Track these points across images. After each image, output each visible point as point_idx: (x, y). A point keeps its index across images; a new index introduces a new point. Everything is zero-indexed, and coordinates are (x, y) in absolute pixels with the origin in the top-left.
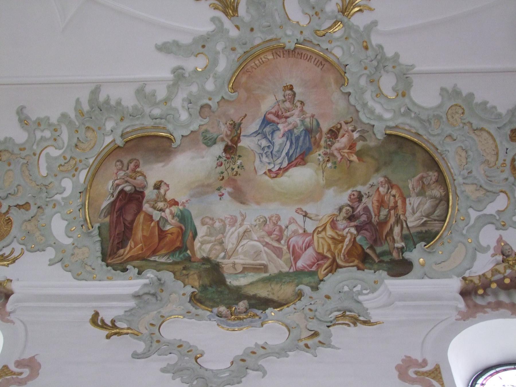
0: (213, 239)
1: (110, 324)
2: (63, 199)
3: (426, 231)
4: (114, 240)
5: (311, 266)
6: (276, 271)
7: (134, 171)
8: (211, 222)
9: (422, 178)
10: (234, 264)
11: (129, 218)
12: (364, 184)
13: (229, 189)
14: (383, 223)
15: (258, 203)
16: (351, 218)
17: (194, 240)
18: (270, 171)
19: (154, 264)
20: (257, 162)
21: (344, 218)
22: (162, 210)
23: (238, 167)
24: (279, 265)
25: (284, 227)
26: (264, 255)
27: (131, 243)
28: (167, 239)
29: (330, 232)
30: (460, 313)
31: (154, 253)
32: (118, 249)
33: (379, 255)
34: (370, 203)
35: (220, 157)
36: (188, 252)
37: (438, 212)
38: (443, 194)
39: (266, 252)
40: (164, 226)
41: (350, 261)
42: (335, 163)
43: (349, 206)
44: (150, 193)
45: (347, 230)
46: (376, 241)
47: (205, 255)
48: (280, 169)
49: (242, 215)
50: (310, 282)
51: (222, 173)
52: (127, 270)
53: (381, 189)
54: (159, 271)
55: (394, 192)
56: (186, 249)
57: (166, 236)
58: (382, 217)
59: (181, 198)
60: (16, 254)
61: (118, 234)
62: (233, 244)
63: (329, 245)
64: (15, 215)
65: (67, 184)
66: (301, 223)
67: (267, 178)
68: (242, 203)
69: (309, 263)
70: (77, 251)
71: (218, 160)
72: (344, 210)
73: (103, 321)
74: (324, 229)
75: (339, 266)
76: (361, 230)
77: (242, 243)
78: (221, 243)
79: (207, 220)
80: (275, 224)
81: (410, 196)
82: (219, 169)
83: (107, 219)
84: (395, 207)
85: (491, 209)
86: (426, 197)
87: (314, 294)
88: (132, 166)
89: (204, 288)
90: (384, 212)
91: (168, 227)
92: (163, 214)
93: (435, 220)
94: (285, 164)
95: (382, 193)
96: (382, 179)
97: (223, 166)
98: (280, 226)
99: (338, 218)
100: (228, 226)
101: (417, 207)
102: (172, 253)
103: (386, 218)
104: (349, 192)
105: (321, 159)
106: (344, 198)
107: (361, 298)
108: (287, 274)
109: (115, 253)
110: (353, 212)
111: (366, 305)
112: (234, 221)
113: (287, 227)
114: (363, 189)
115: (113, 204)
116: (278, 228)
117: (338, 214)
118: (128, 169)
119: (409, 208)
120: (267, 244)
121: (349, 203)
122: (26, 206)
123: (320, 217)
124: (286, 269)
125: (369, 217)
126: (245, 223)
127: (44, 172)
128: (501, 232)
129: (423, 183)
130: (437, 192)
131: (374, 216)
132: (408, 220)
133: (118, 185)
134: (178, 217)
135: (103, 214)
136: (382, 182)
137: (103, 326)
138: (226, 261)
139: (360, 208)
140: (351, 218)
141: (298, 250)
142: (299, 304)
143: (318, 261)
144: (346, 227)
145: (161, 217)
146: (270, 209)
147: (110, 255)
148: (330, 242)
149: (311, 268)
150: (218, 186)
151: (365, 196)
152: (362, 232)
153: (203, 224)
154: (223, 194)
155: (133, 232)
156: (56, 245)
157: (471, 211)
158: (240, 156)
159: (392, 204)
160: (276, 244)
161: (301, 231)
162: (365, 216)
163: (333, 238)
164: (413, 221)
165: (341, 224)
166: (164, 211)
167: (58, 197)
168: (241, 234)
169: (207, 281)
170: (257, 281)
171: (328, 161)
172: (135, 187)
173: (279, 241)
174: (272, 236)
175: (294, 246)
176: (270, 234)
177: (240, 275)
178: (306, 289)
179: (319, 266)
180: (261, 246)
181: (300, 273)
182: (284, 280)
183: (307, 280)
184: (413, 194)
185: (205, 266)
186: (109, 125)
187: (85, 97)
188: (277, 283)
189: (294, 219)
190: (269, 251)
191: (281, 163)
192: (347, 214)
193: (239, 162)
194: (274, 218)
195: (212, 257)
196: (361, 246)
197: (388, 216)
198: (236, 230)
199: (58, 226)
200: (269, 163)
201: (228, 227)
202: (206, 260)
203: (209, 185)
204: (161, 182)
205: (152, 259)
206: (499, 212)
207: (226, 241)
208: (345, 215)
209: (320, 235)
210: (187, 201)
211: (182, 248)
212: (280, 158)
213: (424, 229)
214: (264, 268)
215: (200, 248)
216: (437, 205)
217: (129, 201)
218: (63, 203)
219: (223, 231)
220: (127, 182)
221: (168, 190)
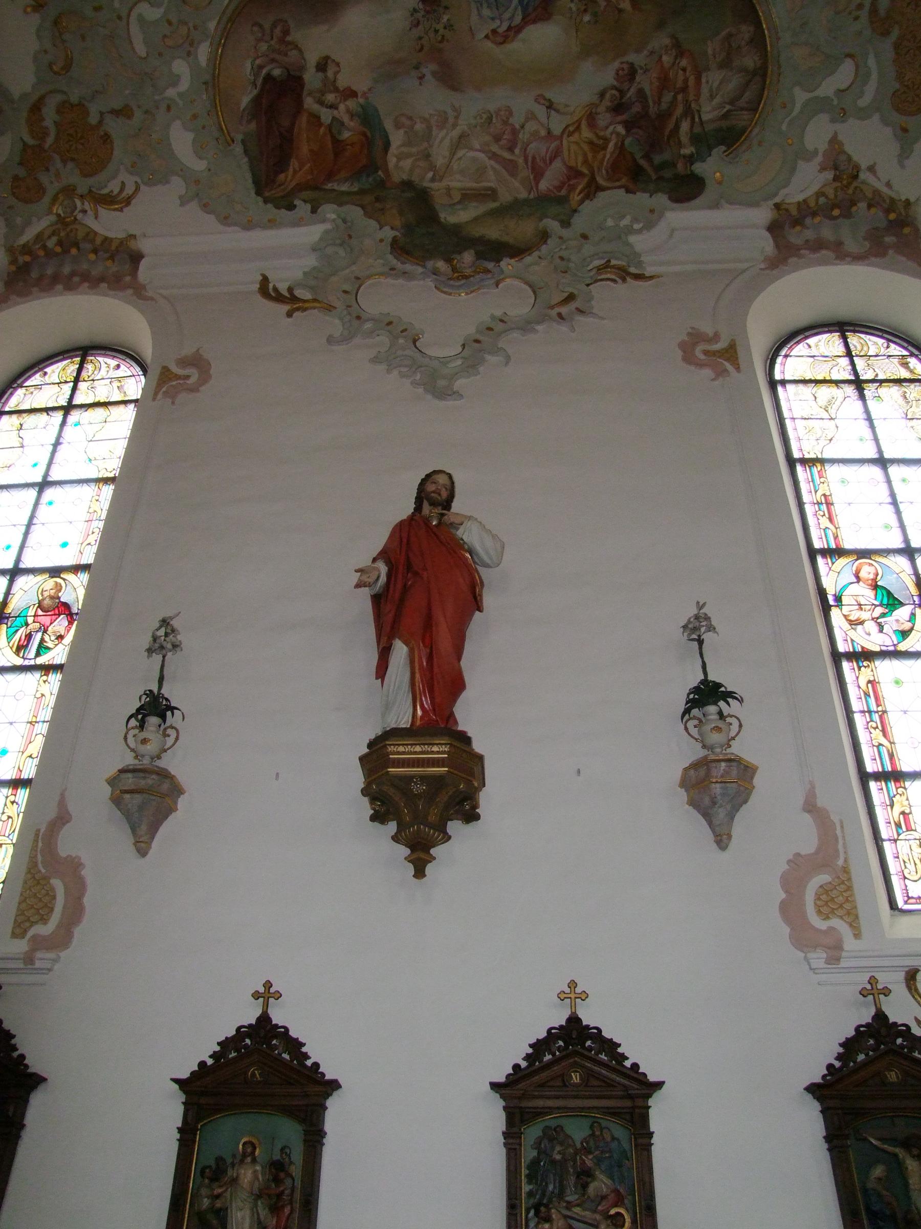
2: (180, 95)
7: (282, 41)
8: (408, 123)
9: (730, 35)
10: (449, 189)
12: (638, 51)
13: (433, 67)
14: (663, 116)
16: (618, 108)
18: (494, 31)
20: (474, 18)
21: (609, 110)
22: (333, 107)
23: (445, 28)
24: (514, 189)
25: (517, 127)
26: (491, 173)
27: (294, 163)
29: (586, 133)
31: (330, 176)
34: (646, 82)
35: (415, 10)
36: (380, 173)
37: (748, 95)
40: (340, 133)
42: (595, 15)
44: (311, 78)
45: (611, 128)
47: (405, 177)
48: (510, 28)
49: (454, 109)
51: (420, 38)
53: (665, 58)
55: (684, 62)
56: (377, 169)
58: (664, 106)
59: (361, 86)
60: (129, 190)
63: (585, 155)
64: (113, 126)
65: (180, 67)
67: (489, 44)
68: (454, 88)
69: (556, 183)
71: (412, 15)
72: (608, 96)
74: (578, 128)
77: (456, 157)
78: (428, 156)
79: (403, 120)
80: (505, 123)
81: (707, 69)
82: (416, 32)
83: (253, 126)
84: (684, 89)
85: (827, 88)
88: (278, 31)
90: (667, 97)
91: (346, 135)
92: (335, 112)
93: (742, 109)
94: (518, 19)
95: (666, 65)
96: (667, 41)
97: (420, 27)
99: (599, 110)
100: (434, 128)
104: (616, 64)
105: (574, 9)
106: (607, 77)
108: (526, 202)
110: (622, 98)
112: (443, 122)
113: (522, 127)
114: (638, 59)
115: (257, 100)
117: (597, 102)
118: (272, 38)
119: (705, 90)
120: (494, 156)
121: (615, 83)
123: (572, 109)
124: (523, 195)
125: (645, 106)
126: (460, 122)
127: (141, 49)
128: (838, 127)
129: (730, 46)
130: (750, 61)
131: (651, 104)
132: (703, 109)
133: (261, 67)
134: (359, 117)
136: (667, 46)
138: (435, 185)
139: (632, 92)
140: (618, 108)
141: (542, 165)
143: (569, 180)
144: (610, 124)
145: (334, 118)
148: (586, 147)
149: (560, 191)
151: (639, 71)
152: (634, 130)
153: (398, 126)
154: (424, 76)
157: (797, 91)
158: (446, 8)
159: (679, 84)
160: (506, 155)
161: (543, 133)
163: (591, 143)
164: (709, 111)
165: (603, 119)
166: (337, 108)
167: (171, 93)
171: (585, 11)
173: (511, 149)
174: (503, 142)
175: (534, 158)
176: (497, 139)
177: (459, 207)
178: (552, 225)
179: (572, 188)
180: (486, 159)
189: (532, 113)
190: (497, 166)
191: (511, 18)
193: (445, 18)
194: (502, 113)
195: (415, 179)
198: (447, 134)
199: (182, 141)
200: (493, 19)
202: (407, 185)
204: (327, 58)
205: (329, 186)
206: (840, 92)
208: (609, 104)
209: (572, 139)
210: (370, 90)
212: (510, 10)
213: (724, 124)
214: (491, 194)
216: (747, 84)
217: (280, 94)
218: (181, 103)
219: (428, 136)
220: (273, 60)
221: (338, 72)
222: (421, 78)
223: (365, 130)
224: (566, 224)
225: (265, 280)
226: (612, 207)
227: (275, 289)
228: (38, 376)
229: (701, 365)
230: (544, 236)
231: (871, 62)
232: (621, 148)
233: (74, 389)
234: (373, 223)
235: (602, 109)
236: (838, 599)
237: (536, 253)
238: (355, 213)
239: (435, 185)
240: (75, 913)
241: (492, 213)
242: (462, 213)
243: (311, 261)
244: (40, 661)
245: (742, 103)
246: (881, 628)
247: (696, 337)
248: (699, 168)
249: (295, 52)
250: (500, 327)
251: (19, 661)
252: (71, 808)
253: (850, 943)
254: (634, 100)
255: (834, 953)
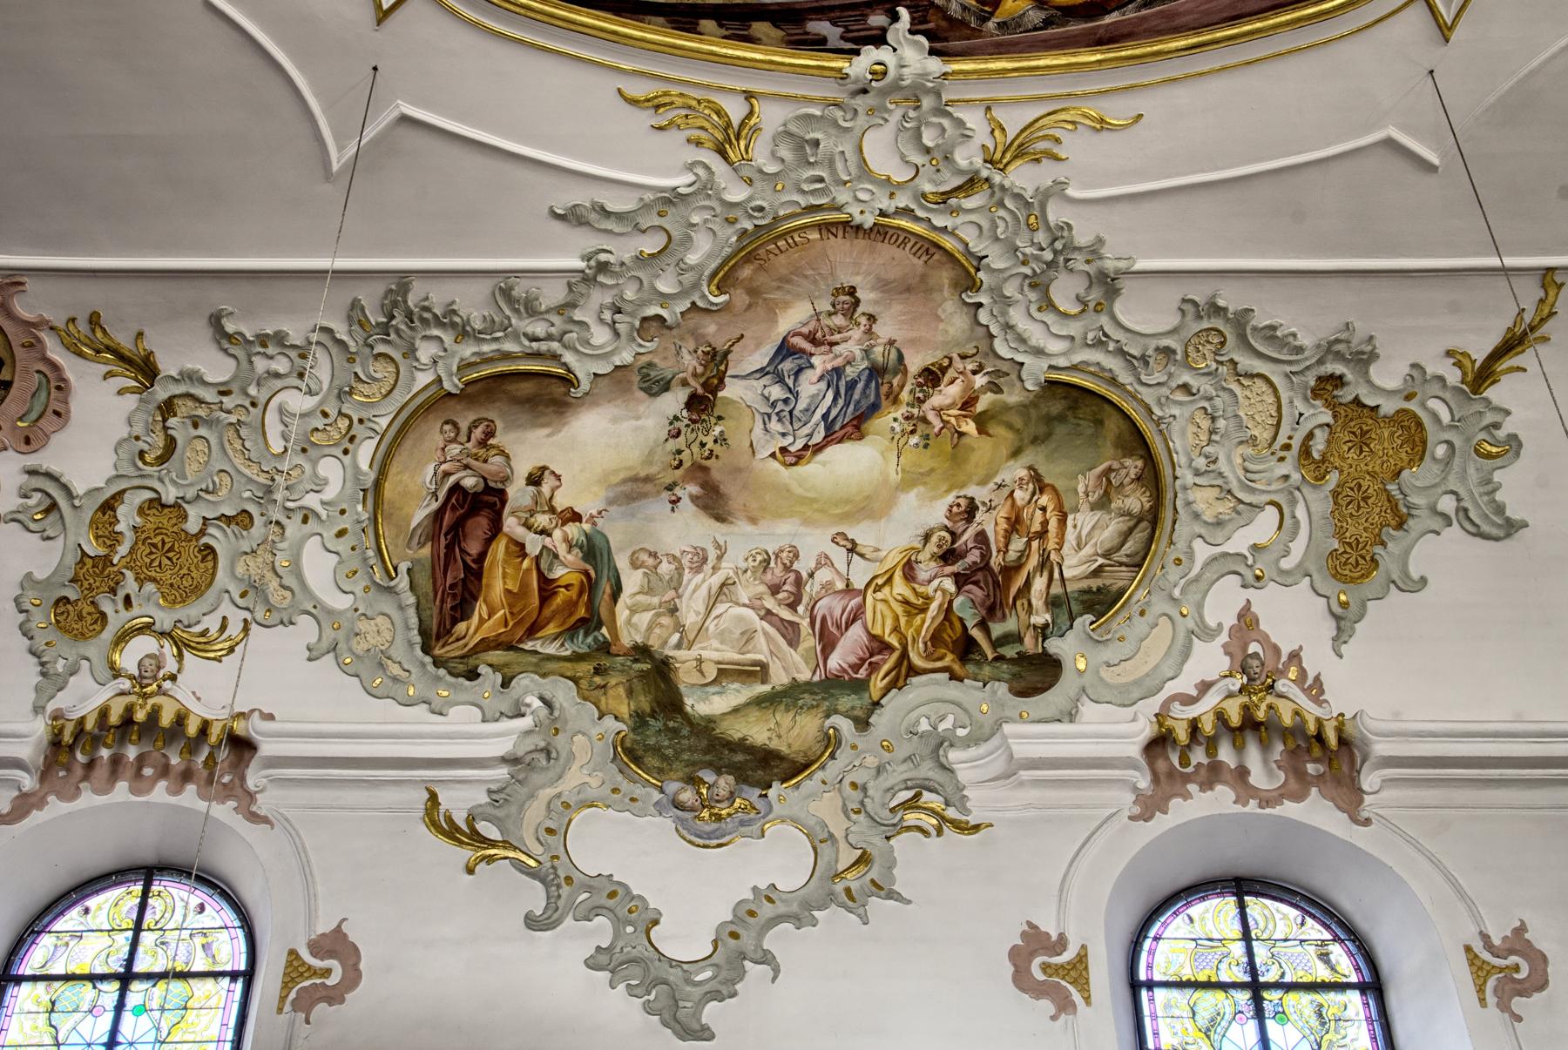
0: (656, 600)
1: (464, 827)
3: (1099, 589)
4: (443, 601)
5: (856, 667)
6: (786, 680)
7: (483, 443)
8: (651, 561)
10: (700, 661)
11: (473, 548)
14: (1010, 570)
15: (753, 520)
17: (615, 601)
19: (533, 659)
21: (933, 557)
22: (544, 532)
24: (793, 665)
25: (805, 575)
26: (762, 640)
27: (480, 608)
28: (559, 600)
29: (900, 587)
30: (1140, 797)
31: (532, 631)
32: (455, 622)
33: (996, 644)
34: (991, 523)
36: (604, 630)
37: (1129, 547)
38: (1147, 506)
39: (766, 634)
40: (550, 570)
41: (936, 655)
43: (946, 529)
44: (518, 493)
45: (936, 583)
46: (992, 610)
49: (718, 547)
50: (853, 708)
52: (479, 675)
54: (544, 676)
55: (1044, 500)
56: (600, 625)
57: (556, 593)
59: (586, 506)
61: (452, 586)
62: (698, 613)
63: (897, 618)
64: (217, 538)
66: (842, 568)
68: (720, 519)
69: (853, 659)
70: (363, 626)
72: (934, 539)
73: (449, 820)
74: (889, 581)
75: (913, 671)
76: (965, 583)
77: (715, 613)
78: (673, 611)
79: (644, 557)
80: (787, 569)
81: (1076, 510)
82: (673, 445)
83: (426, 551)
84: (1042, 534)
86: (1110, 512)
87: (861, 742)
89: (639, 720)
90: (1018, 544)
91: (559, 572)
92: (548, 540)
93: (1121, 564)
98: (797, 573)
99: (920, 557)
101: (1089, 534)
102: (571, 632)
103: (1020, 558)
106: (937, 513)
107: (953, 755)
108: (808, 687)
109: (449, 632)
110: (953, 542)
111: (964, 774)
113: (811, 575)
115: (438, 515)
116: (792, 576)
119: (1070, 535)
121: (947, 522)
122: (243, 519)
124: (804, 675)
125: (986, 556)
126: (724, 565)
130: (1136, 501)
131: (994, 553)
133: (447, 474)
135: (416, 540)
137: (451, 832)
138: (681, 654)
141: (833, 630)
143: (871, 655)
144: (935, 577)
145: (544, 547)
146: (777, 534)
147: (438, 638)
148: (899, 609)
150: (668, 481)
153: (635, 565)
154: (679, 499)
155: (484, 581)
156: (319, 613)
159: (1036, 527)
160: (786, 614)
161: (840, 585)
162: (977, 552)
163: (906, 602)
164: (1075, 566)
166: (550, 535)
168: (714, 590)
169: (645, 703)
170: (747, 705)
172: (485, 479)
173: (793, 606)
174: (781, 596)
175: (824, 619)
176: (775, 590)
177: (711, 689)
178: (845, 725)
179: (874, 668)
181: (832, 686)
182: (800, 703)
183: (847, 701)
184: (1084, 507)
185: (637, 666)
186: (426, 352)
187: (370, 297)
188: (787, 710)
189: (827, 557)
192: (939, 546)
194: (784, 555)
195: (654, 643)
196: (961, 620)
197: (1024, 554)
198: (704, 581)
199: (319, 566)
201: (687, 575)
202: (642, 651)
203: (648, 479)
204: (544, 469)
205: (528, 646)
207: (682, 605)
209: (879, 595)
211: (591, 623)
213: (1094, 583)
214: (759, 672)
215: (629, 622)
216: (1131, 531)
217: (472, 510)
218: (323, 514)
219: (676, 583)
220: (467, 467)
222: (674, 502)
223: (588, 567)
224: (863, 724)
230: (831, 742)
232: (949, 610)
235: (924, 556)
239: (681, 654)
241: (760, 702)
242: (716, 698)
245: (1120, 556)
249: (498, 459)
254: (970, 545)
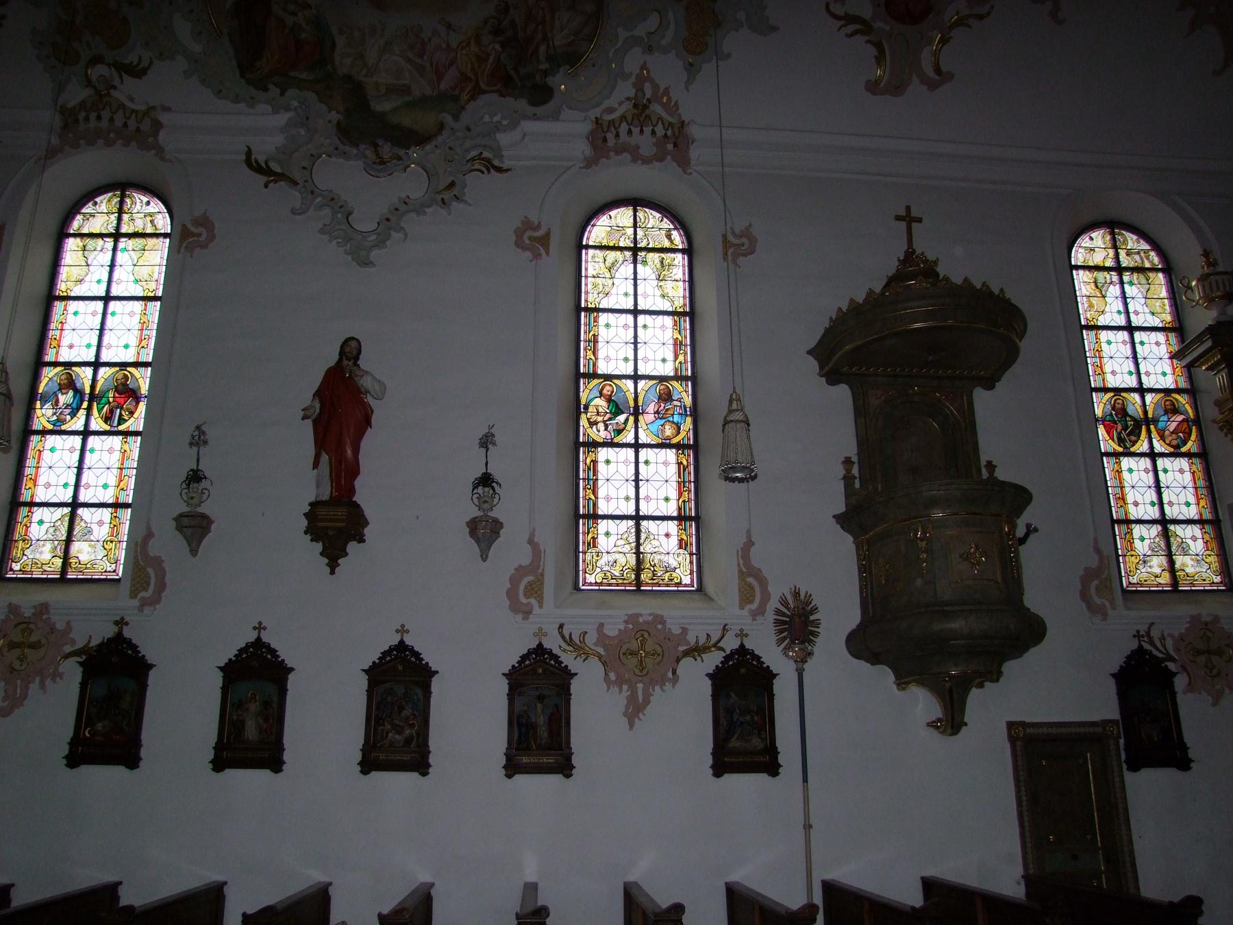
29: (474, 48)
91: (304, 36)
120: (409, 61)
140: (497, 32)
142: (440, 139)
157: (620, 30)
160: (419, 61)
178: (448, 119)
205: (292, 74)
214: (406, 90)
224: (456, 118)
225: (249, 153)
226: (487, 108)
227: (256, 161)
228: (90, 204)
229: (525, 248)
231: (671, 15)
233: (119, 220)
234: (324, 107)
236: (586, 407)
237: (434, 143)
238: (311, 96)
240: (161, 586)
243: (280, 140)
244: (121, 428)
246: (606, 427)
247: (528, 225)
248: (550, 80)
250: (403, 208)
251: (108, 428)
252: (154, 530)
253: (536, 610)
255: (527, 613)
